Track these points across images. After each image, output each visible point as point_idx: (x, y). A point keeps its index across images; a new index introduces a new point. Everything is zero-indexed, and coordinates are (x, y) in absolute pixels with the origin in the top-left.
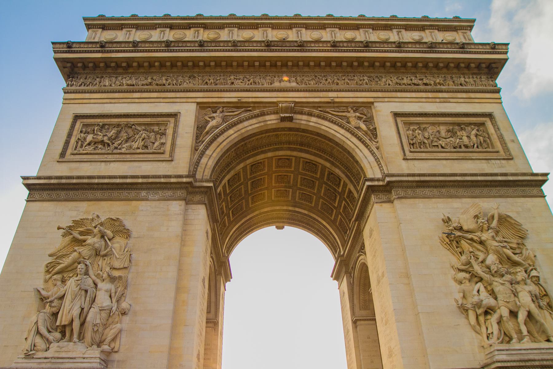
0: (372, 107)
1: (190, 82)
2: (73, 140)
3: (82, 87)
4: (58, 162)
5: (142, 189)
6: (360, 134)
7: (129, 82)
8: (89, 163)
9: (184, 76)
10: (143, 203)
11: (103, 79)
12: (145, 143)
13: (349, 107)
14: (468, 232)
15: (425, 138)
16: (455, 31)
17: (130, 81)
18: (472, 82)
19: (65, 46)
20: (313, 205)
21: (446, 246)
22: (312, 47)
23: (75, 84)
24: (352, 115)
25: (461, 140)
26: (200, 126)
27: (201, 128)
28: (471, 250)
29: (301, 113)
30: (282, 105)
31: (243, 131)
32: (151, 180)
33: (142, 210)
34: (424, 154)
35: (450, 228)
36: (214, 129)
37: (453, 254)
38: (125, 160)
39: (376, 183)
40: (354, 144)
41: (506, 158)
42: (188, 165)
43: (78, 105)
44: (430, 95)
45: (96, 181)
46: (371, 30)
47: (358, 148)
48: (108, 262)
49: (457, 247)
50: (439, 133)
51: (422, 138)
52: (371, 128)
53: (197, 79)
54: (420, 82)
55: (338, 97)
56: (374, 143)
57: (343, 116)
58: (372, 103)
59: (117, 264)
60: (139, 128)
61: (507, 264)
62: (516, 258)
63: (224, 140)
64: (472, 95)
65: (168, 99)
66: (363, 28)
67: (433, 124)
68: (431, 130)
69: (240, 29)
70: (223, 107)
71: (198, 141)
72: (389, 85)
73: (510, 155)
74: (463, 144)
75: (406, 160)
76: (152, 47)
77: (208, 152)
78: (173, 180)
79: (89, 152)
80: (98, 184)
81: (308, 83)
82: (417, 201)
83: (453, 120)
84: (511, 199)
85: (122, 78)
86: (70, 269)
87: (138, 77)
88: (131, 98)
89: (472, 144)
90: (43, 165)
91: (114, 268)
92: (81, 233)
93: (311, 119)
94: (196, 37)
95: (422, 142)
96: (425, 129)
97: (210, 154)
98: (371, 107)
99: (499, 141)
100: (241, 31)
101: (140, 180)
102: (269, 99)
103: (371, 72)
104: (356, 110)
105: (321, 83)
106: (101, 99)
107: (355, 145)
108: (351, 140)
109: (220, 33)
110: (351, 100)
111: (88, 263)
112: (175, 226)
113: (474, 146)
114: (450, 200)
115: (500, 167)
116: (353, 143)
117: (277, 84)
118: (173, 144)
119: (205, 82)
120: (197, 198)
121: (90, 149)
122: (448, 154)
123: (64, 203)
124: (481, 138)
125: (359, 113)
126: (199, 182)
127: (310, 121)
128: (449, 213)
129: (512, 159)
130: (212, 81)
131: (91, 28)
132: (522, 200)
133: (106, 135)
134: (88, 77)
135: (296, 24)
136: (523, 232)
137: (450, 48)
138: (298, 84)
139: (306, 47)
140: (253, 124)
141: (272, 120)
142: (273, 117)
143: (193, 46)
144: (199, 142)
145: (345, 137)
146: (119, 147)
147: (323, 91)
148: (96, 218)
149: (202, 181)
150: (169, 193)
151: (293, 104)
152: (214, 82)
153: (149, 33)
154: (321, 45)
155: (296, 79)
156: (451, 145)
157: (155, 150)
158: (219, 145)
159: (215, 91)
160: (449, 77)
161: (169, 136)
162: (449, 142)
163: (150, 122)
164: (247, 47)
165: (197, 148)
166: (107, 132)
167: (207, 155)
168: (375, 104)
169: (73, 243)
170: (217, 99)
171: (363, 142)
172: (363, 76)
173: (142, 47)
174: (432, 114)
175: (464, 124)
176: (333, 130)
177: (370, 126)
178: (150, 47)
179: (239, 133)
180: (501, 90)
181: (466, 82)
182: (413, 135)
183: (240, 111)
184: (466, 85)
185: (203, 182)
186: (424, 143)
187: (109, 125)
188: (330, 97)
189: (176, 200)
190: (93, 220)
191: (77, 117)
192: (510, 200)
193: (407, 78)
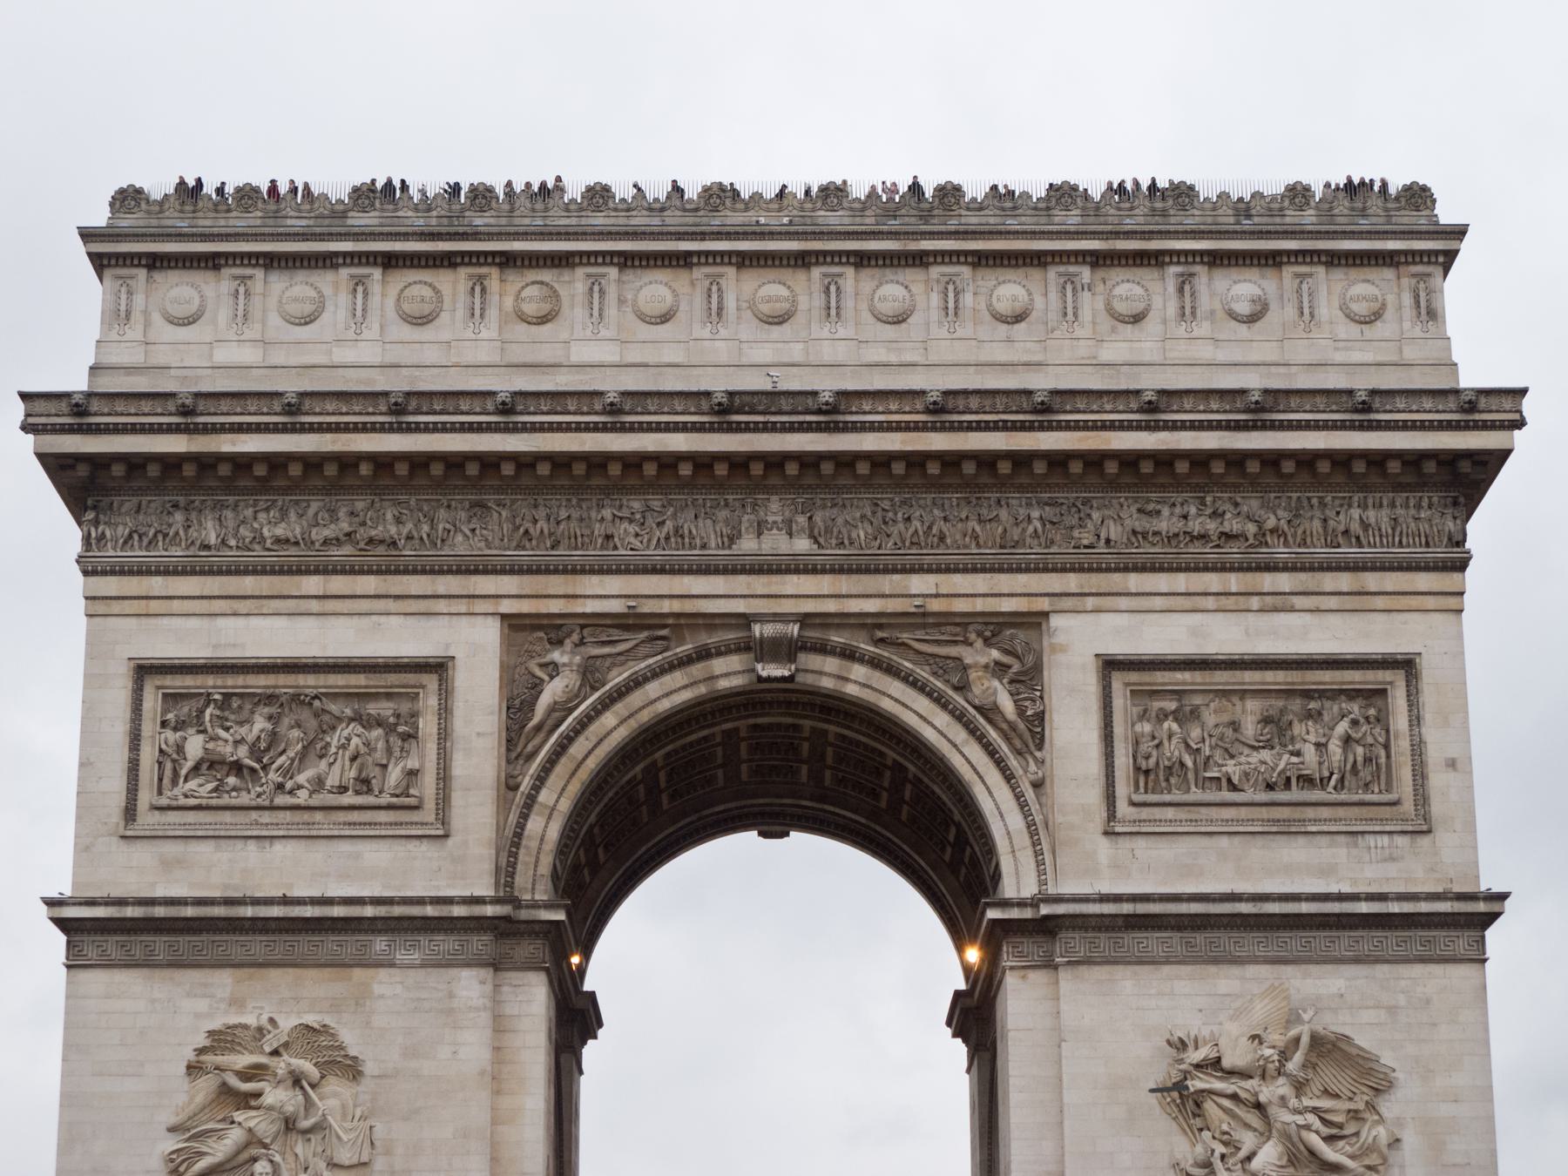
0: (1044, 627)
1: (473, 530)
2: (148, 756)
3: (137, 554)
4: (122, 837)
5: (373, 932)
6: (993, 734)
7: (280, 531)
8: (212, 843)
9: (453, 503)
10: (383, 973)
11: (194, 515)
12: (360, 771)
13: (971, 628)
14: (1231, 1073)
15: (1188, 746)
16: (1391, 265)
17: (283, 525)
18: (1386, 526)
19: (64, 406)
20: (883, 804)
21: (1169, 1111)
22: (865, 413)
23: (108, 533)
24: (978, 655)
25: (1294, 759)
26: (517, 702)
27: (520, 710)
28: (1225, 1127)
29: (823, 649)
30: (761, 634)
31: (645, 716)
32: (398, 911)
33: (382, 997)
34: (1170, 813)
35: (1183, 1067)
36: (557, 714)
37: (1186, 1134)
38: (314, 833)
39: (1014, 914)
40: (972, 766)
41: (1410, 828)
42: (494, 852)
43: (133, 620)
44: (1234, 581)
45: (249, 912)
46: (1085, 273)
47: (983, 781)
48: (320, 1149)
49: (1195, 1115)
50: (1235, 730)
51: (1176, 753)
52: (1029, 713)
53: (495, 515)
54: (1212, 526)
55: (937, 596)
56: (1033, 767)
57: (949, 658)
58: (1046, 615)
59: (345, 1156)
60: (333, 707)
61: (1307, 1167)
62: (1330, 1153)
63: (590, 753)
64: (1372, 581)
65: (411, 601)
66: (1061, 263)
67: (1225, 694)
68: (1215, 711)
69: (626, 265)
70: (583, 627)
71: (514, 755)
72: (1108, 541)
73: (1426, 818)
74: (1297, 773)
75: (1113, 837)
76: (347, 414)
77: (545, 796)
78: (458, 911)
79: (204, 802)
80: (253, 919)
81: (850, 538)
82: (1120, 971)
83: (1290, 680)
84: (1386, 968)
85: (256, 512)
86: (228, 1166)
87: (305, 504)
88: (296, 597)
89: (1326, 774)
90: (84, 848)
91: (336, 1165)
92: (245, 1075)
93: (849, 671)
94: (477, 312)
95: (1177, 765)
96: (1195, 714)
97: (551, 804)
98: (1040, 624)
99: (1410, 763)
100: (629, 275)
101: (369, 911)
102: (723, 601)
103: (1057, 485)
104: (993, 636)
105: (888, 536)
106: (202, 597)
107: (975, 770)
108: (966, 750)
109: (556, 285)
110: (980, 605)
111: (277, 1158)
112: (473, 1047)
113: (1330, 778)
114: (1212, 969)
115: (1385, 860)
116: (969, 762)
117: (748, 544)
118: (444, 777)
119: (522, 530)
120: (527, 949)
121: (201, 787)
122: (1244, 812)
123: (167, 973)
124: (1360, 750)
125: (998, 649)
126: (528, 907)
127: (847, 680)
128: (1200, 1011)
129: (1429, 831)
130: (542, 524)
131: (109, 266)
132: (1418, 970)
133: (241, 741)
134: (144, 503)
135: (825, 253)
136: (1382, 1076)
137: (1324, 412)
138: (816, 542)
139: (844, 413)
140: (675, 691)
141: (729, 672)
142: (734, 662)
143: (478, 410)
144: (517, 758)
145: (949, 740)
146: (289, 785)
147: (895, 570)
148: (270, 1028)
149: (535, 905)
150: (447, 944)
151: (795, 622)
152: (551, 534)
153: (313, 294)
154: (893, 407)
155: (810, 518)
156: (1260, 778)
157: (394, 800)
158: (576, 770)
159: (556, 571)
160: (1315, 501)
161: (429, 745)
162: (1255, 769)
163: (366, 687)
164: (655, 413)
165: (511, 782)
166: (241, 723)
167: (541, 804)
168: (1056, 621)
169: (223, 1097)
170: (562, 601)
171: (1001, 764)
172: (1029, 505)
173: (315, 414)
174: (1223, 662)
175: (1322, 694)
176: (915, 712)
177: (1027, 703)
178: (341, 414)
179: (633, 724)
180: (1472, 562)
181: (1365, 526)
182: (1154, 738)
183: (634, 642)
184: (1362, 538)
185: (539, 907)
186: (1182, 764)
187: (241, 695)
188: (915, 596)
189: (468, 965)
190: (260, 1029)
191: (144, 671)
192: (1382, 970)
193: (1174, 505)
